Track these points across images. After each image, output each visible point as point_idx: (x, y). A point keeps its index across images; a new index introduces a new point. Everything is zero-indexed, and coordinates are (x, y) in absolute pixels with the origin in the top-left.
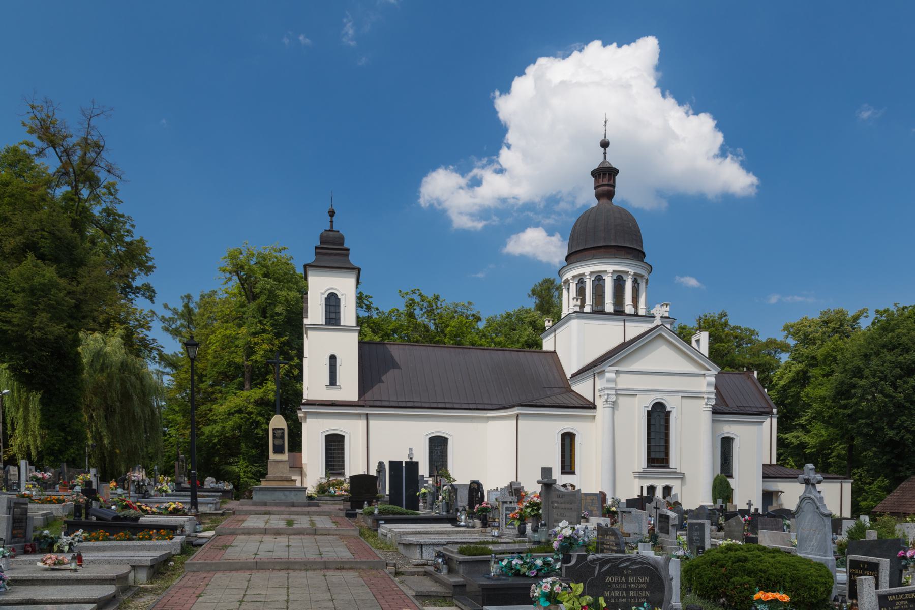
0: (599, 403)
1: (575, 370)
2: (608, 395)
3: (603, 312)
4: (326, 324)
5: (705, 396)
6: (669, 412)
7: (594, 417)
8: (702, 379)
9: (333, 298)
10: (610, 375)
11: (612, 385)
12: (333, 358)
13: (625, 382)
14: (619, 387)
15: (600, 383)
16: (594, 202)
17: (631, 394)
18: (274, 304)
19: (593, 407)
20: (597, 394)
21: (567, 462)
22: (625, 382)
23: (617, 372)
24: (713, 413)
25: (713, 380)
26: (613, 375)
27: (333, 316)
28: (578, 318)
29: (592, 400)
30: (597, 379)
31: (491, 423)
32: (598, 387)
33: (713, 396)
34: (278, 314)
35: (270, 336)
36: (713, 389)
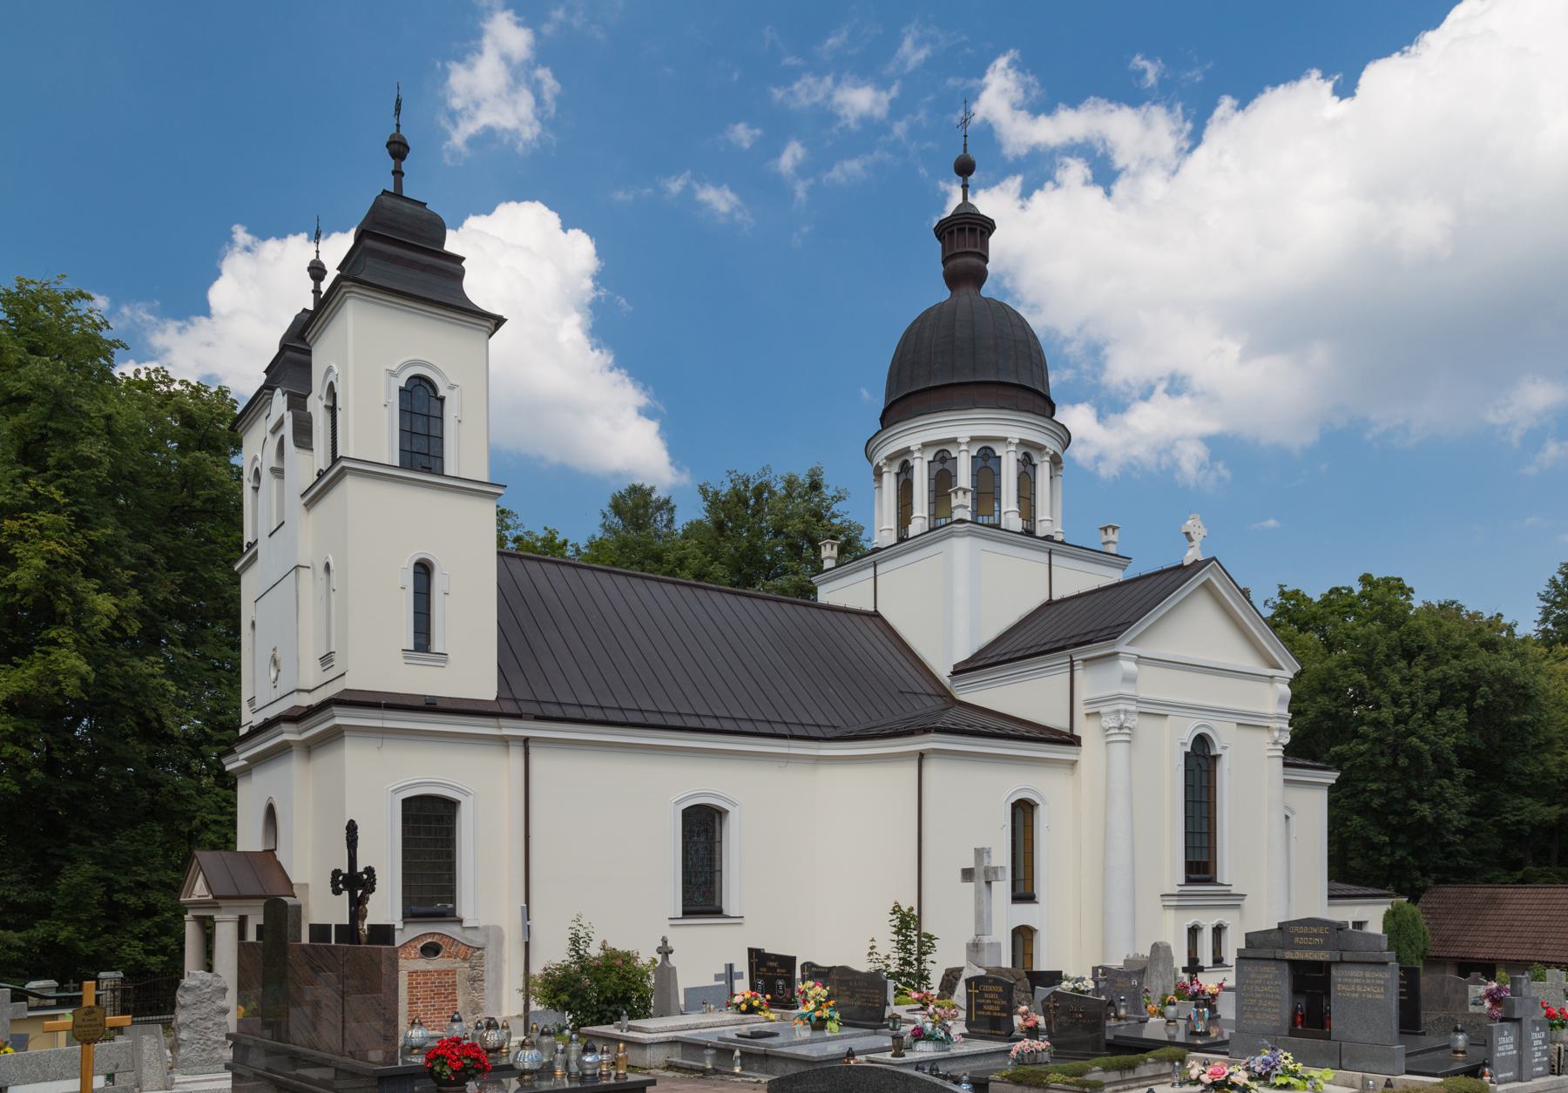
0: (1083, 728)
1: (963, 654)
2: (1126, 712)
3: (997, 527)
4: (403, 466)
5: (1276, 725)
6: (1216, 758)
7: (1074, 763)
8: (1264, 687)
9: (420, 392)
10: (1128, 666)
11: (1127, 690)
12: (423, 570)
13: (1156, 685)
14: (1143, 695)
15: (1090, 684)
16: (943, 294)
17: (1155, 711)
18: (67, 437)
19: (1073, 740)
20: (1080, 710)
21: (1021, 875)
22: (1156, 685)
23: (1140, 659)
24: (1285, 765)
25: (1287, 691)
26: (1128, 666)
27: (420, 444)
28: (971, 534)
29: (1061, 723)
30: (1077, 674)
31: (825, 774)
32: (1082, 694)
33: (1286, 726)
34: (86, 463)
35: (63, 519)
36: (1284, 711)
